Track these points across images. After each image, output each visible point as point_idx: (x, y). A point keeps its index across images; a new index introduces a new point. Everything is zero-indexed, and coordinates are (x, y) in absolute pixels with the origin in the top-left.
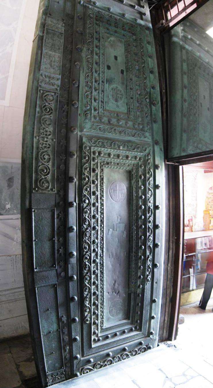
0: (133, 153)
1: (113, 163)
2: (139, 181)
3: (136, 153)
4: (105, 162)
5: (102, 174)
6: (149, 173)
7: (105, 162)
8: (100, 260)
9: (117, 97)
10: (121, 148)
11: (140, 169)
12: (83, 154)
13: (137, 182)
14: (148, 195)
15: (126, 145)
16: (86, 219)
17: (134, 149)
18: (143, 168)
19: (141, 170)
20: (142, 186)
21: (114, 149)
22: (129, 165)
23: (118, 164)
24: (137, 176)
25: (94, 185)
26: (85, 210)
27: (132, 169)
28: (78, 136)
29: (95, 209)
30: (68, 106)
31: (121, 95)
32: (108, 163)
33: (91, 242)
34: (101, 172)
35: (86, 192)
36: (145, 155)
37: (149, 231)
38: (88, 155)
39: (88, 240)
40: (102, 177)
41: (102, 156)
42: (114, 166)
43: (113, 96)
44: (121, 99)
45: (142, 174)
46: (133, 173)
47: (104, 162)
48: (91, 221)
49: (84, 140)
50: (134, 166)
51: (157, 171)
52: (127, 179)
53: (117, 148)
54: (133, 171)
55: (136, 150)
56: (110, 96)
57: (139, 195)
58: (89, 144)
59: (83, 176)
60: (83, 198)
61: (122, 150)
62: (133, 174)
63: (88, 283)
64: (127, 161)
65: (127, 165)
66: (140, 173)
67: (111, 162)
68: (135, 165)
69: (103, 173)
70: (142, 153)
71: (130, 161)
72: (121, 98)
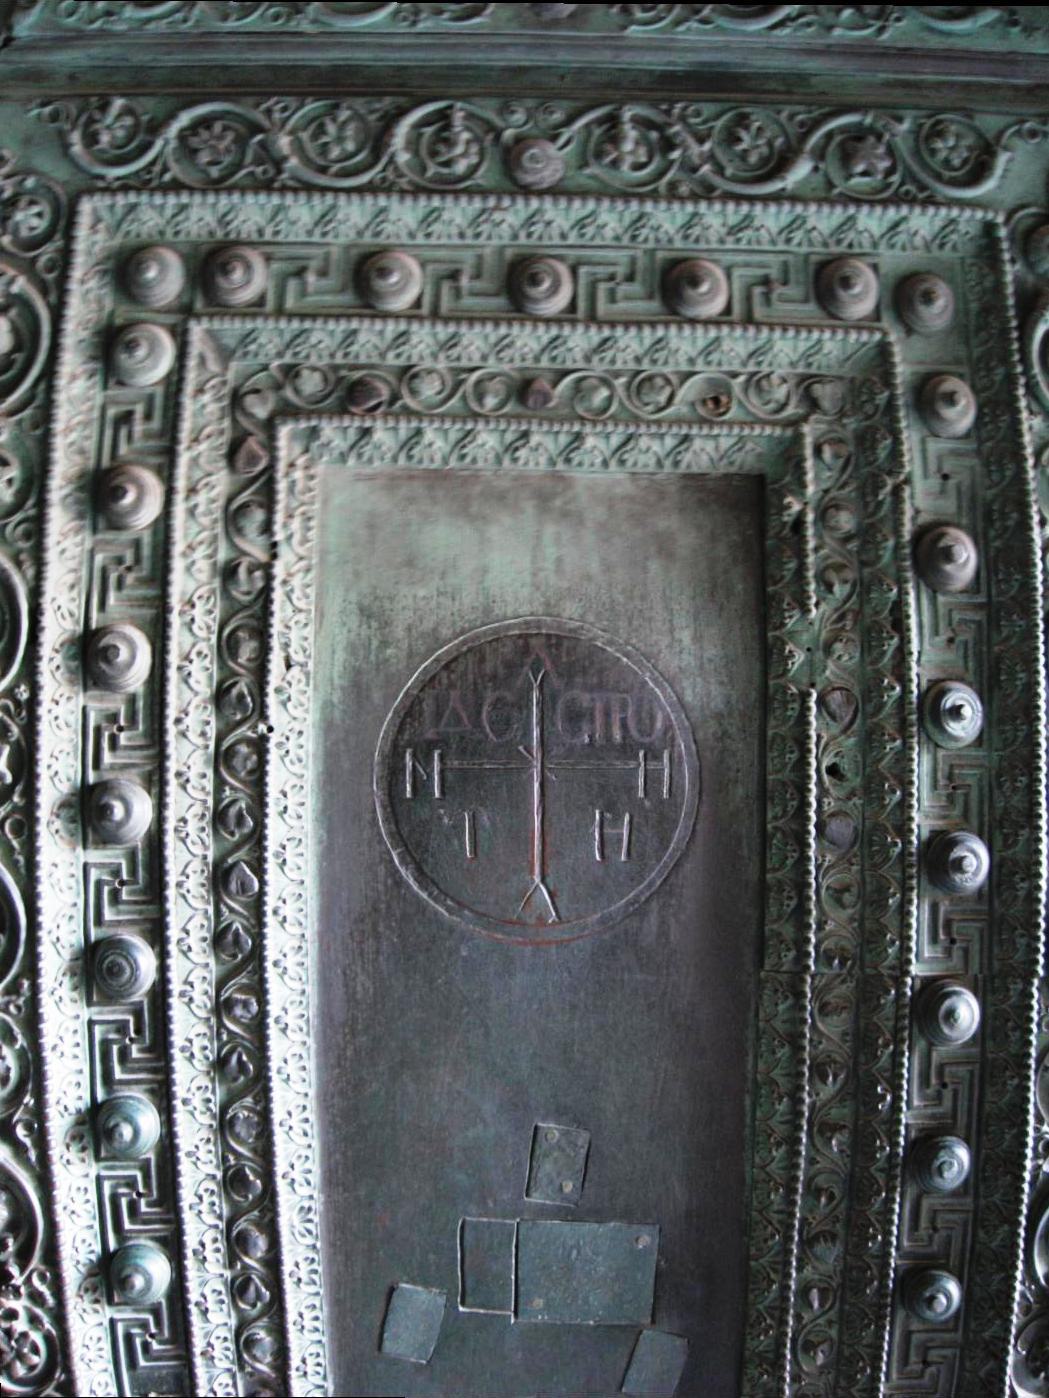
0: (770, 219)
1: (429, 389)
2: (899, 624)
3: (823, 220)
4: (311, 383)
5: (256, 549)
7: (311, 383)
10: (549, 162)
11: (911, 437)
13: (869, 642)
15: (631, 134)
17: (779, 164)
18: (961, 415)
19: (933, 446)
20: (962, 696)
21: (417, 191)
22: (716, 399)
23: (523, 390)
25: (99, 705)
27: (789, 456)
29: (121, 1028)
34: (233, 518)
36: (989, 228)
40: (246, 584)
41: (260, 301)
42: (455, 431)
45: (949, 506)
47: (291, 372)
50: (813, 404)
52: (713, 590)
54: (800, 472)
57: (903, 829)
61: (556, 191)
62: (799, 523)
64: (684, 343)
65: (688, 391)
66: (921, 499)
68: (825, 393)
69: (267, 528)
70: (930, 201)
71: (736, 345)
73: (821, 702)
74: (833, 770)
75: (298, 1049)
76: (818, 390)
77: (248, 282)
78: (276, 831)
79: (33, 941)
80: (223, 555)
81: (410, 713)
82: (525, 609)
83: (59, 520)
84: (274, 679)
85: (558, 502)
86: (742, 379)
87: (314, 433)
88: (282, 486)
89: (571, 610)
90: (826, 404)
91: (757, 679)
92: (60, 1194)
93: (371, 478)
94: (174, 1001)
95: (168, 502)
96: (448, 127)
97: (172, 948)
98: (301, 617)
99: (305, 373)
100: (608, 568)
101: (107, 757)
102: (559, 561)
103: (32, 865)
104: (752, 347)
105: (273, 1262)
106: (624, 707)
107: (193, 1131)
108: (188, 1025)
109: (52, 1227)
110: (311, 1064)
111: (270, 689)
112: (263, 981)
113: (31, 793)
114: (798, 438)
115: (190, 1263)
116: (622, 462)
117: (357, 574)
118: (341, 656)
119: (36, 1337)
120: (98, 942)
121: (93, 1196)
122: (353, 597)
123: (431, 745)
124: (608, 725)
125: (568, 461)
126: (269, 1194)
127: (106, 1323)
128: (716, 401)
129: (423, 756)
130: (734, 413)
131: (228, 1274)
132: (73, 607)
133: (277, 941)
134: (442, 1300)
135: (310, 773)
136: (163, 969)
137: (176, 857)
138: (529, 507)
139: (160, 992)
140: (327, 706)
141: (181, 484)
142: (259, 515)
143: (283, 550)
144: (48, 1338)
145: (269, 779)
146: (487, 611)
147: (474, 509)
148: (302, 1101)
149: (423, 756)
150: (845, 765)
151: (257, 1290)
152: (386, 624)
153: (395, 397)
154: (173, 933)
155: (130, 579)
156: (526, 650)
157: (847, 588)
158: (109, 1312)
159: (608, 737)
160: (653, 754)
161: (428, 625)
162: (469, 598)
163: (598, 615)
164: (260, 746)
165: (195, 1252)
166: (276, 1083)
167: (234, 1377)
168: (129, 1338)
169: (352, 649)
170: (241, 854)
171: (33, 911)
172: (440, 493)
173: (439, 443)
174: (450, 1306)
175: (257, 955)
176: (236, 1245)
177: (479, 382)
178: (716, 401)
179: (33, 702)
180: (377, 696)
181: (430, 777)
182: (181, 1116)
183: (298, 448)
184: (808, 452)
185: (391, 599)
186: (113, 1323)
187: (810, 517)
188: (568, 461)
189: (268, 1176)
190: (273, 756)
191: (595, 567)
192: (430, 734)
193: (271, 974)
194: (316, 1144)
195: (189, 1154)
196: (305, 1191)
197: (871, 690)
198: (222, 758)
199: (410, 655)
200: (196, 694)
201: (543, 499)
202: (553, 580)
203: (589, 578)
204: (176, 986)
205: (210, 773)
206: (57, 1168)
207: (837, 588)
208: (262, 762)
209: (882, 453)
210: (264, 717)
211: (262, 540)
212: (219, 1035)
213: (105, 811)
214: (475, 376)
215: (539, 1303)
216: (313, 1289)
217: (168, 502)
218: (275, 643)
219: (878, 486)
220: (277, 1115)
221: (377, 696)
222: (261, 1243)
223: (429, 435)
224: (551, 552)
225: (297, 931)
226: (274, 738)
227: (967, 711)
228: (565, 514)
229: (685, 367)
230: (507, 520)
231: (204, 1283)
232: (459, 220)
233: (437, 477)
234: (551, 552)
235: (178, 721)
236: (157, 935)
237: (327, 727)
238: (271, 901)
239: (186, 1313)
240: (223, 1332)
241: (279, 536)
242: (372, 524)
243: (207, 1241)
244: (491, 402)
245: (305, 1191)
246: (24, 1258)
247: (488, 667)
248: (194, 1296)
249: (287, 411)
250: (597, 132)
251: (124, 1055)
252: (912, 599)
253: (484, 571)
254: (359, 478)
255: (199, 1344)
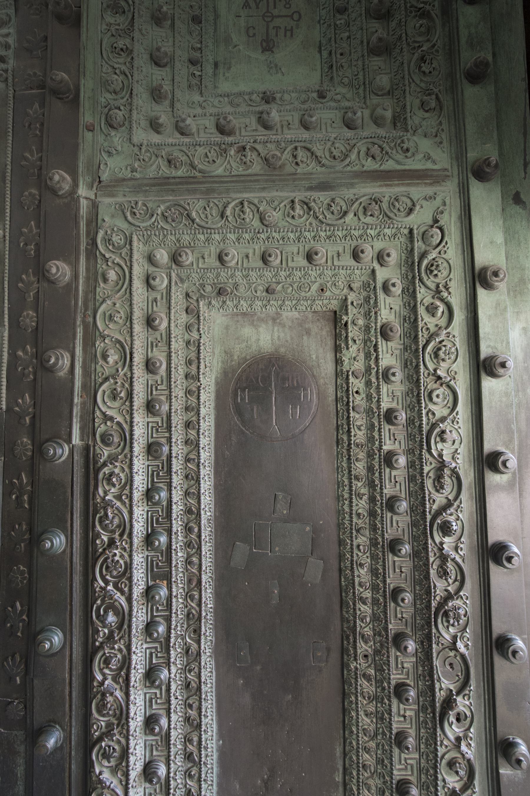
1: (242, 289)
5: (195, 335)
6: (431, 310)
7: (208, 288)
8: (186, 669)
9: (272, 32)
12: (99, 266)
14: (431, 407)
16: (107, 504)
24: (367, 328)
26: (106, 470)
28: (84, 203)
30: (42, 105)
31: (291, 17)
32: (220, 292)
33: (129, 600)
34: (188, 328)
35: (117, 404)
37: (443, 573)
38: (118, 264)
39: (116, 586)
43: (251, 33)
44: (292, 36)
46: (345, 318)
47: (203, 286)
48: (131, 513)
49: (105, 214)
51: (481, 292)
53: (256, 223)
54: (347, 310)
55: (351, 215)
56: (233, 36)
58: (124, 226)
59: (100, 345)
60: (99, 426)
62: (346, 324)
63: (114, 771)
65: (315, 287)
67: (236, 286)
68: (355, 286)
69: (198, 330)
72: (292, 30)
73: (353, 373)
74: (357, 392)
75: (208, 472)
76: (353, 285)
77: (188, 259)
78: (203, 411)
79: (131, 443)
80: (186, 337)
81: (239, 379)
82: (270, 351)
83: (138, 328)
84: (202, 371)
85: (278, 321)
86: (330, 283)
87: (210, 303)
88: (202, 318)
89: (282, 350)
90: (355, 289)
91: (334, 368)
92: (135, 516)
93: (227, 315)
94: (173, 459)
95: (169, 323)
96: (243, 207)
97: (173, 444)
98: (209, 354)
99: (206, 286)
100: (292, 338)
101: (154, 393)
102: (279, 336)
103: (132, 422)
104: (333, 273)
105: (199, 536)
106: (297, 377)
107: (177, 495)
108: (177, 465)
109: (131, 526)
110: (212, 477)
111: (201, 373)
112: (199, 453)
113: (131, 402)
114: (346, 299)
115: (173, 537)
116: (296, 309)
117: (224, 342)
118: (220, 364)
119: (122, 562)
120: (151, 444)
121: (145, 516)
122: (223, 348)
123: (246, 388)
124: (293, 381)
125: (281, 309)
126: (199, 515)
127: (145, 556)
128: (322, 290)
129: (243, 390)
130: (328, 293)
131: (185, 540)
132: (143, 352)
133: (203, 441)
134: (248, 548)
135: (213, 396)
136: (170, 450)
137: (175, 420)
138: (270, 322)
139: (170, 457)
140: (216, 378)
141: (172, 318)
142: (196, 326)
143: (203, 335)
144: (126, 563)
145: (201, 398)
146: (259, 351)
147: (255, 323)
148: (209, 487)
149: (243, 390)
150: (361, 391)
151: (193, 545)
152: (232, 356)
153: (232, 292)
154: (174, 440)
155: (159, 344)
156: (270, 361)
157: (361, 341)
158: (147, 553)
159: (293, 384)
160: (305, 389)
161: (243, 355)
162: (254, 347)
163: (290, 352)
164: (199, 388)
165: (175, 533)
166: (202, 482)
167: (184, 575)
168: (152, 561)
169: (223, 362)
170: (194, 419)
171: (131, 435)
172: (246, 319)
173: (245, 305)
174: (251, 549)
175: (198, 445)
176: (188, 530)
177: (255, 288)
178: (322, 290)
179: (132, 378)
180: (230, 375)
181: (245, 396)
182: (174, 492)
183: (206, 308)
184: (349, 303)
185: (233, 348)
186: (147, 556)
187: (349, 322)
188: (281, 309)
189: (199, 510)
190: (202, 391)
191: (289, 338)
192: (245, 385)
193: (202, 451)
194: (213, 500)
195: (175, 503)
196: (209, 514)
197: (368, 370)
198: (188, 392)
199: (239, 364)
200: (180, 375)
201: (274, 320)
202: (277, 342)
203: (287, 341)
204: (174, 455)
205: (184, 396)
206: (135, 508)
207: (357, 342)
208: (199, 393)
209: (372, 302)
210: (199, 381)
211: (197, 333)
212: (186, 468)
213: (153, 407)
214: (254, 285)
215: (277, 549)
216: (210, 544)
217: (169, 323)
218: (202, 361)
219: (370, 312)
220: (202, 491)
221: (230, 375)
222: (196, 530)
223: (242, 302)
224: (276, 334)
225: (208, 439)
226: (202, 386)
227: (397, 374)
228: (280, 324)
229: (313, 280)
230: (264, 326)
231: (177, 543)
232: (247, 237)
233: (244, 314)
234: (276, 334)
235: (175, 382)
236: (169, 440)
237: (217, 383)
238: (201, 431)
239: (171, 552)
240: (182, 559)
241: (202, 332)
242: (227, 328)
243: (179, 529)
244: (259, 292)
245: (209, 514)
246: (121, 535)
247: (260, 366)
248: (174, 547)
249: (202, 296)
250: (288, 207)
251: (158, 475)
252: (380, 343)
253: (259, 340)
254: (223, 315)
255: (174, 563)
